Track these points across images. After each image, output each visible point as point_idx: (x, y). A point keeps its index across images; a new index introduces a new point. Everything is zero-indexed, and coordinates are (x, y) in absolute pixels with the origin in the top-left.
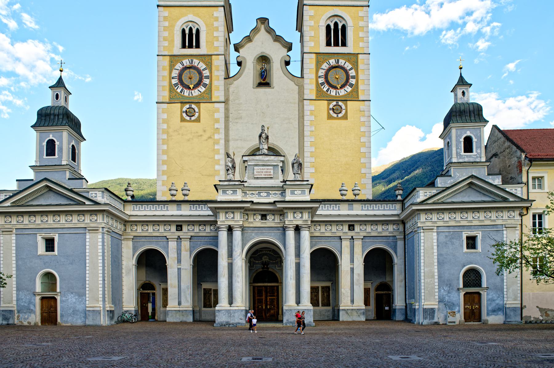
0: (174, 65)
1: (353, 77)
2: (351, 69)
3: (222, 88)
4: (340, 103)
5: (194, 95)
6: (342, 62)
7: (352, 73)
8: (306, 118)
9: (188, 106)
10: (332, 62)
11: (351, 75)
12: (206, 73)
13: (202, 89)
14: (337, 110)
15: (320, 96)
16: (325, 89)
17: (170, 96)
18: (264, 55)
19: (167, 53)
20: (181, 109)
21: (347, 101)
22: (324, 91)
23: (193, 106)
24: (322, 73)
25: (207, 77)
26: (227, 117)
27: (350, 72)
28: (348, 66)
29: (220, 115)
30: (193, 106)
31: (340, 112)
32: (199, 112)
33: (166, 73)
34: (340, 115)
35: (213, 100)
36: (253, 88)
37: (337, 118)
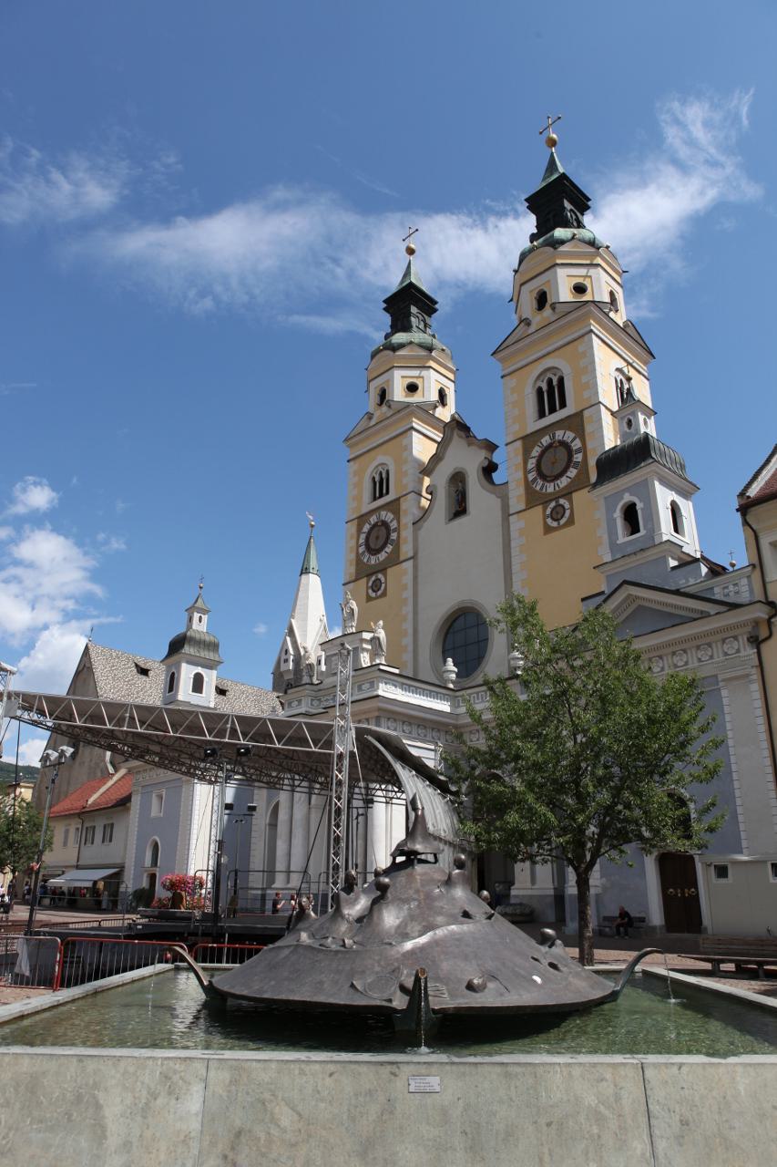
0: (362, 529)
1: (578, 451)
2: (574, 439)
3: (410, 539)
4: (562, 501)
5: (381, 559)
6: (559, 434)
7: (577, 444)
8: (513, 544)
9: (373, 578)
10: (546, 440)
11: (574, 448)
12: (394, 525)
13: (389, 548)
14: (557, 514)
15: (533, 499)
16: (538, 488)
17: (357, 570)
18: (457, 471)
19: (355, 516)
20: (367, 583)
21: (571, 493)
22: (536, 491)
23: (380, 576)
24: (532, 464)
25: (395, 530)
26: (415, 578)
27: (572, 445)
28: (569, 436)
29: (408, 579)
30: (380, 576)
31: (554, 519)
32: (386, 582)
33: (353, 543)
34: (562, 522)
35: (402, 558)
36: (446, 524)
37: (559, 528)
